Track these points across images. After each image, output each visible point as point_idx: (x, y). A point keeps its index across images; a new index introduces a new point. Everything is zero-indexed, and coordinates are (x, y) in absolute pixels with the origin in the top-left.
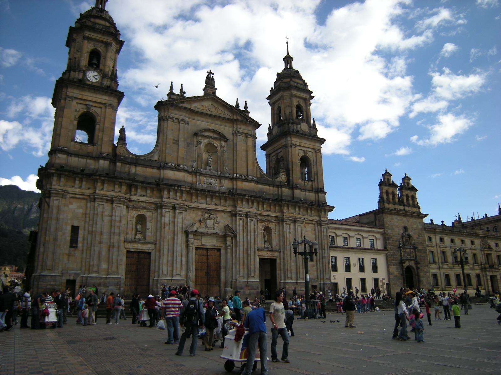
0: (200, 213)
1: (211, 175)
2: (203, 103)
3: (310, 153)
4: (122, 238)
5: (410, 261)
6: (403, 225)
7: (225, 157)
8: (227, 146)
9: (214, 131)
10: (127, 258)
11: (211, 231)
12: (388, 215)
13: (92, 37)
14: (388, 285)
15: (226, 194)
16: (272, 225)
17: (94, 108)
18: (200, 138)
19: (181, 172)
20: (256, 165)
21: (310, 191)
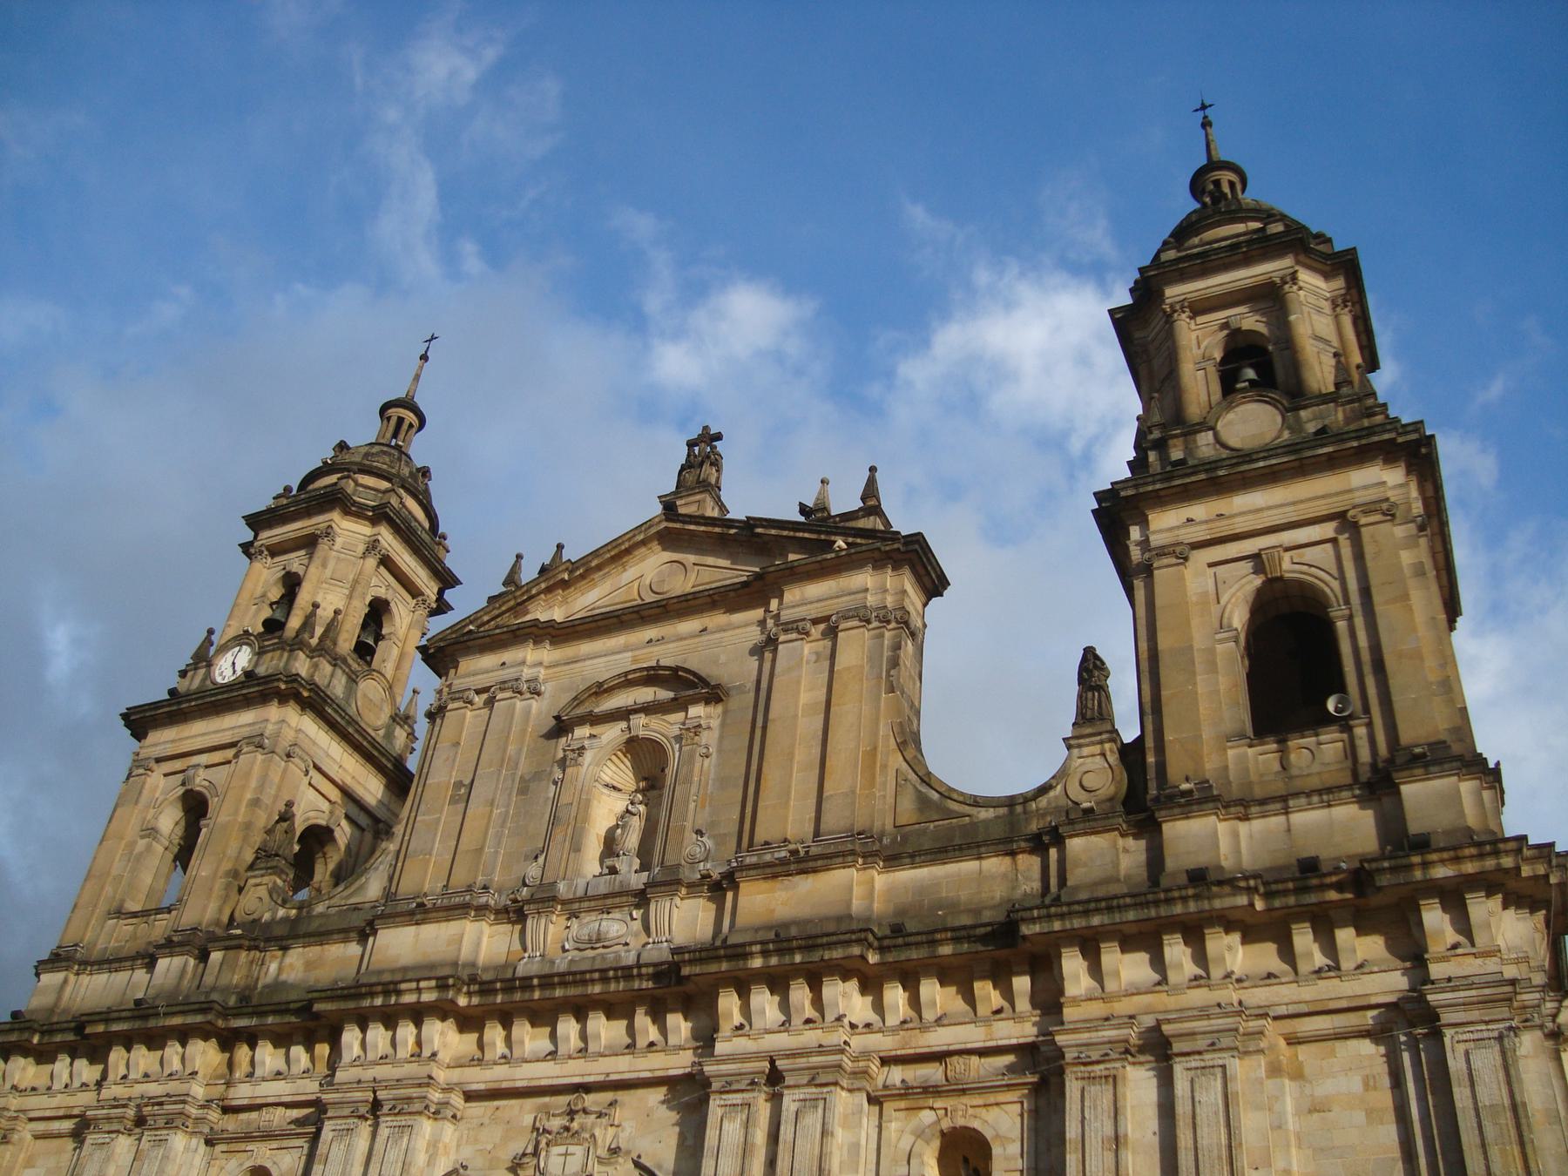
1: (606, 896)
3: (1309, 555)
8: (723, 725)
9: (652, 676)
16: (992, 1115)
20: (897, 761)
21: (1326, 794)
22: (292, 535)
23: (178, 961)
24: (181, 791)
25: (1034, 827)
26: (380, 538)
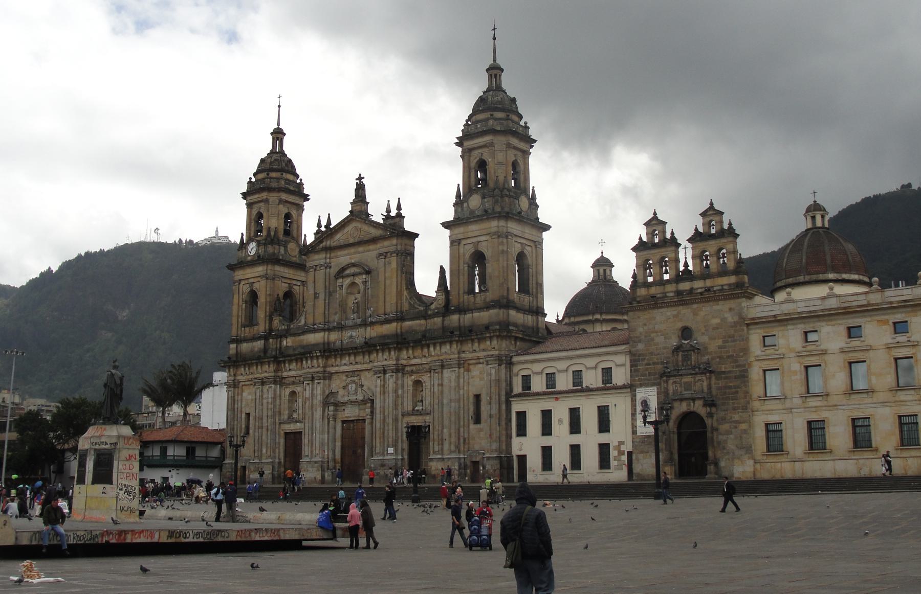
0: (344, 378)
2: (346, 230)
3: (484, 244)
4: (277, 420)
5: (692, 401)
6: (680, 325)
7: (368, 296)
9: (354, 265)
10: (285, 439)
11: (354, 398)
12: (640, 314)
13: (252, 201)
14: (630, 454)
15: (359, 349)
16: (423, 377)
17: (255, 285)
18: (340, 280)
19: (320, 332)
20: (405, 293)
21: (480, 309)
22: (256, 200)
23: (263, 342)
24: (249, 290)
25: (430, 312)
26: (282, 197)
